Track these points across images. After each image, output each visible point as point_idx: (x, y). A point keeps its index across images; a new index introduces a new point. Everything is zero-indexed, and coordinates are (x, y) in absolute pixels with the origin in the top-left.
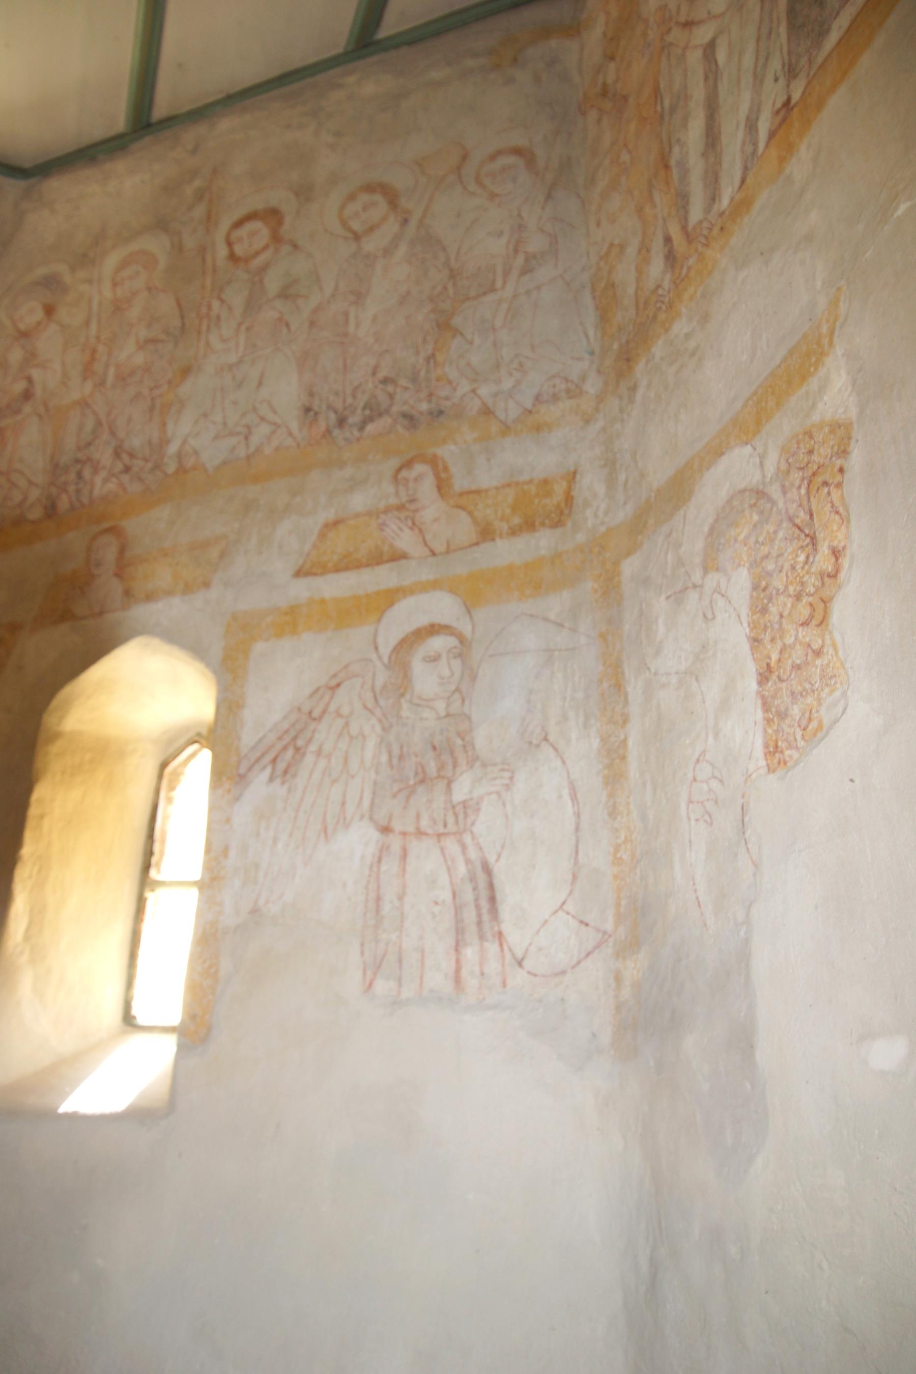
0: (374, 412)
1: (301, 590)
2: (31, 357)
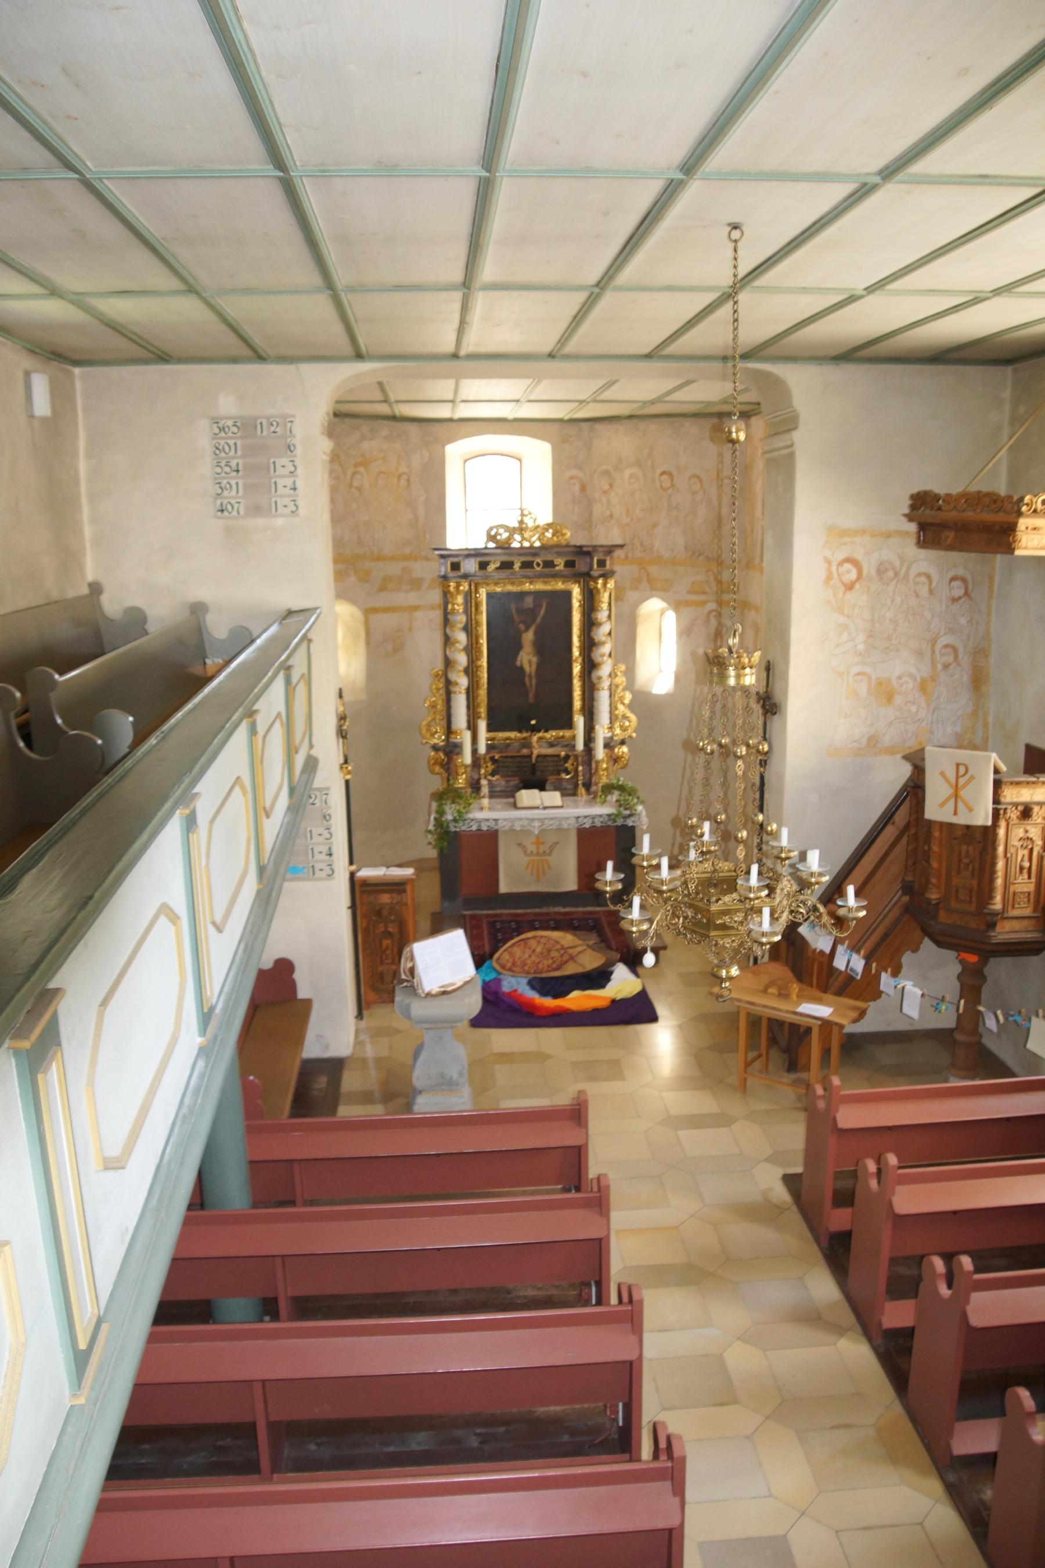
0: (700, 554)
1: (690, 597)
2: (609, 502)
